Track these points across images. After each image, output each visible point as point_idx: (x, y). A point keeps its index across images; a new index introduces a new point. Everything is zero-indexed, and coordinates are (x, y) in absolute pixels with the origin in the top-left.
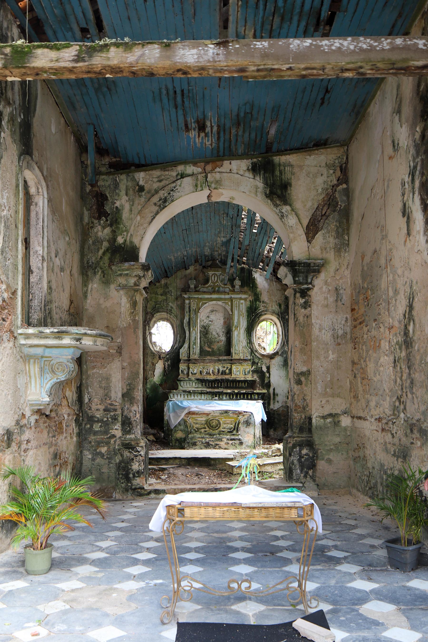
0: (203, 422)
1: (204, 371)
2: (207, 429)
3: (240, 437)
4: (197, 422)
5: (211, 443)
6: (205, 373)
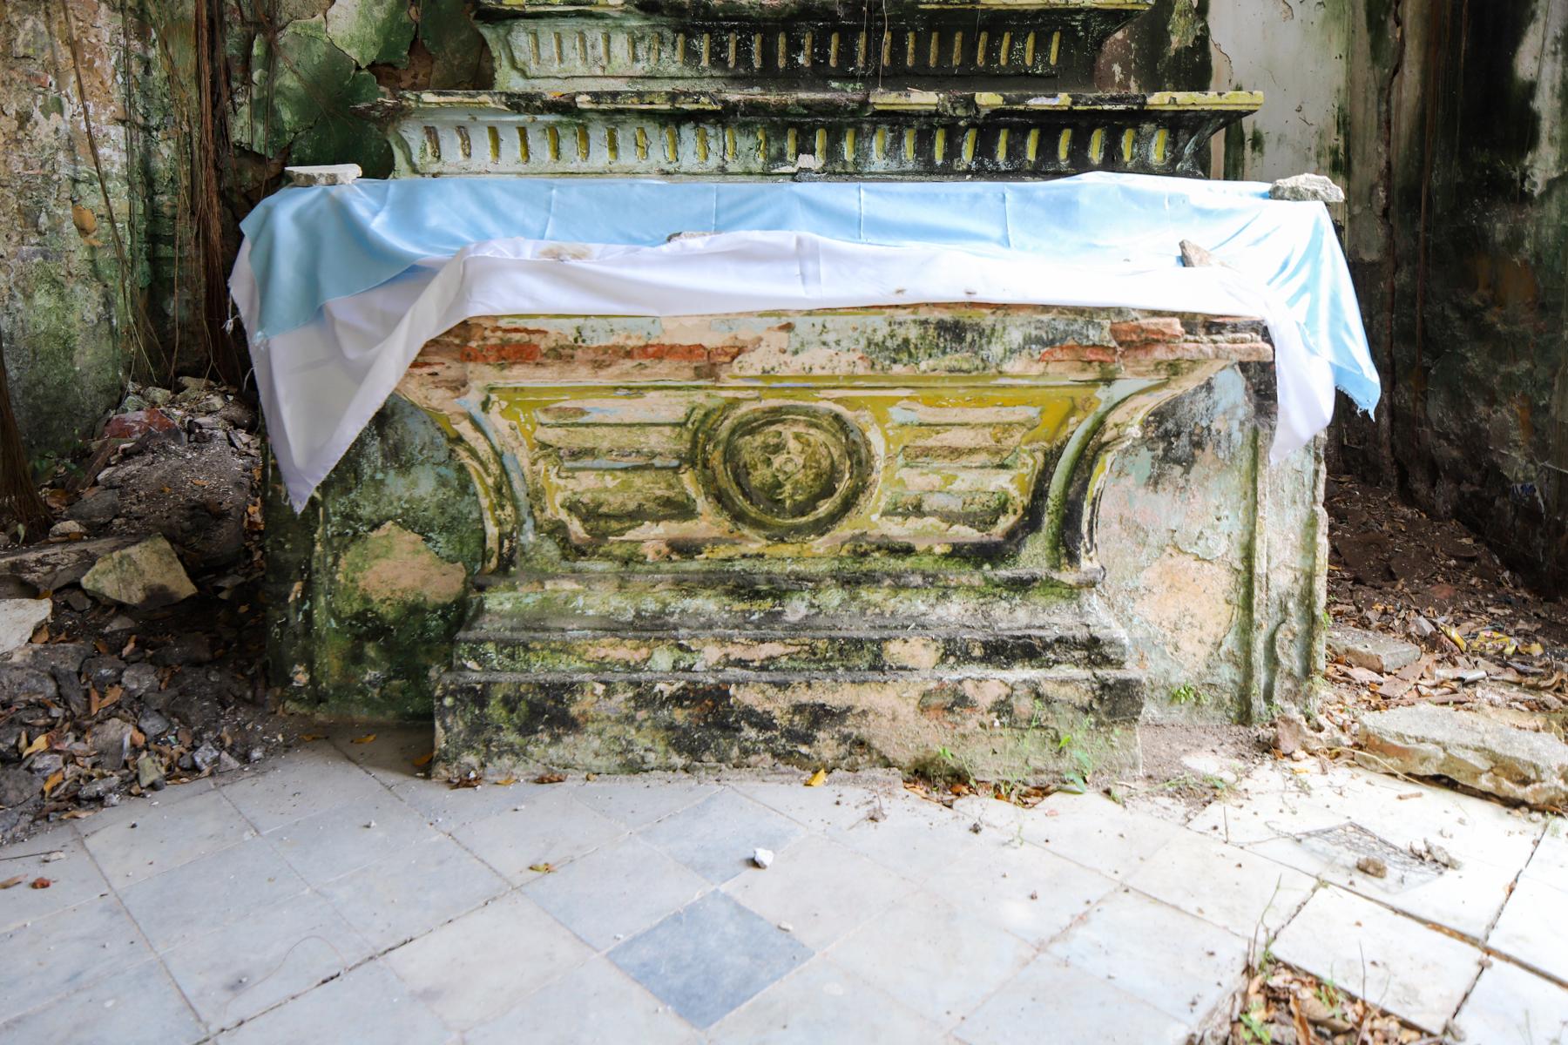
0: (655, 440)
2: (707, 523)
3: (1101, 618)
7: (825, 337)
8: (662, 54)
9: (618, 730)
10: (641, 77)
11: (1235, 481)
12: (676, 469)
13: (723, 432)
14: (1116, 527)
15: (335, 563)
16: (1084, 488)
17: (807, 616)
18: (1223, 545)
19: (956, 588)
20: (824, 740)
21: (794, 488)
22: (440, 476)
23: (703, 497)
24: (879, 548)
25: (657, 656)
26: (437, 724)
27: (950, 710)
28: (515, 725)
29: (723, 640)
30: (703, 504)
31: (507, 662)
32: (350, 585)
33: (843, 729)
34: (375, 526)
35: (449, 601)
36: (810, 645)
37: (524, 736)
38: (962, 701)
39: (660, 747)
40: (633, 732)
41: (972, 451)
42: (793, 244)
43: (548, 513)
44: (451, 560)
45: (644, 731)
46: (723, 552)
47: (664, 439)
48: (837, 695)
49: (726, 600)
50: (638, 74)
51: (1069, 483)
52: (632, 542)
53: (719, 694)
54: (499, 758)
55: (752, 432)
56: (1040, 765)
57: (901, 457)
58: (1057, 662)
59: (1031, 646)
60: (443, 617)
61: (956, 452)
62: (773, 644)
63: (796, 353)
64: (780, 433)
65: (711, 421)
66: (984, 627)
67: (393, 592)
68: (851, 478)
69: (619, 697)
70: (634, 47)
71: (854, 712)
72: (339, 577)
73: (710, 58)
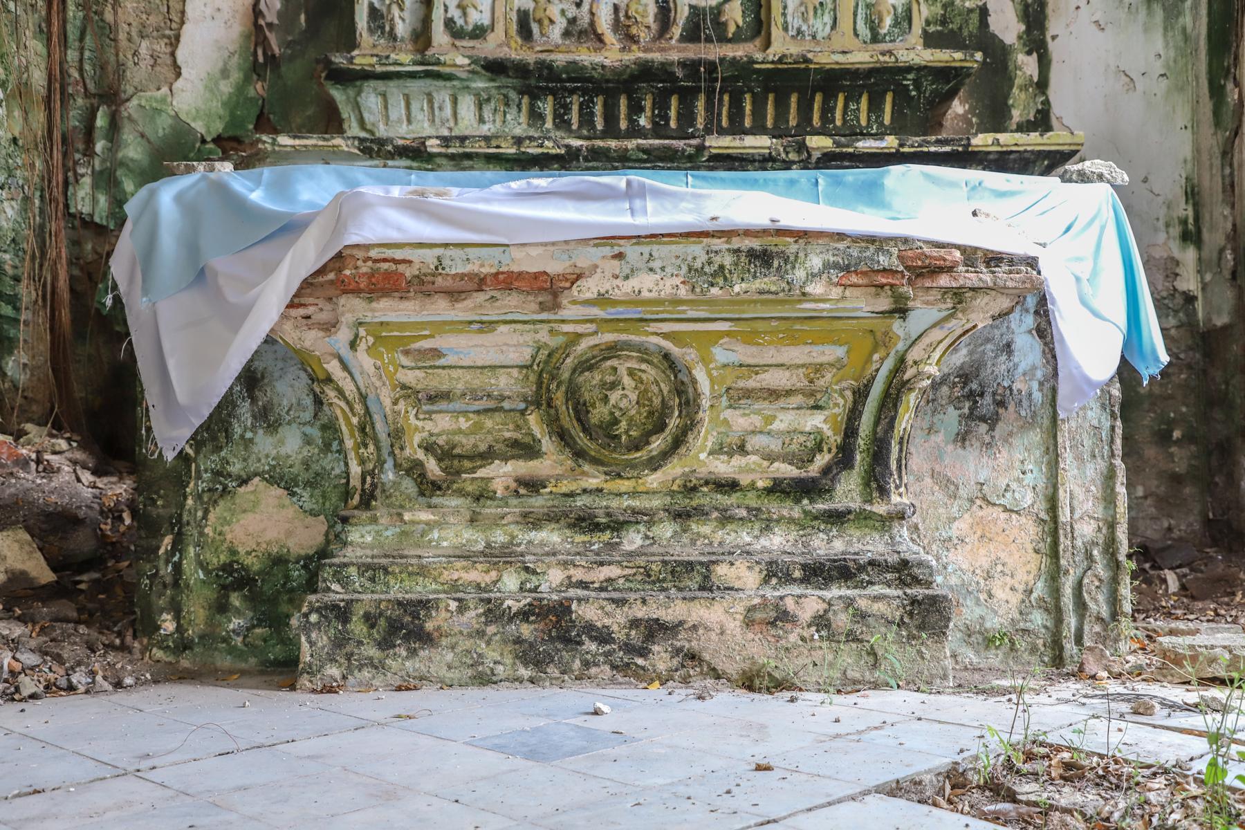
0: (505, 383)
4: (440, 381)
5: (589, 612)
6: (556, 33)
7: (651, 264)
8: (508, 116)
9: (468, 644)
11: (1035, 437)
12: (523, 412)
13: (566, 375)
14: (928, 480)
15: (205, 517)
16: (891, 426)
17: (642, 546)
18: (1029, 499)
19: (778, 521)
20: (659, 653)
21: (628, 425)
22: (305, 435)
23: (547, 438)
24: (707, 483)
25: (505, 578)
26: (303, 639)
27: (773, 624)
28: (375, 640)
29: (565, 564)
30: (547, 444)
31: (368, 584)
32: (218, 538)
33: (675, 643)
34: (244, 482)
35: (311, 552)
36: (645, 568)
37: (383, 650)
38: (783, 617)
39: (508, 660)
40: (483, 645)
41: (789, 393)
42: (623, 185)
43: (408, 452)
44: (313, 513)
45: (494, 645)
46: (565, 487)
47: (513, 381)
48: (670, 611)
49: (568, 532)
51: (877, 422)
52: (482, 479)
53: (562, 610)
54: (360, 670)
55: (590, 368)
56: (857, 675)
57: (725, 398)
58: (871, 583)
59: (847, 568)
60: (305, 567)
61: (774, 394)
62: (611, 567)
63: (627, 278)
64: (615, 369)
65: (554, 361)
66: (803, 553)
67: (258, 544)
68: (680, 416)
69: (472, 613)
70: (480, 109)
71: (686, 626)
72: (206, 530)
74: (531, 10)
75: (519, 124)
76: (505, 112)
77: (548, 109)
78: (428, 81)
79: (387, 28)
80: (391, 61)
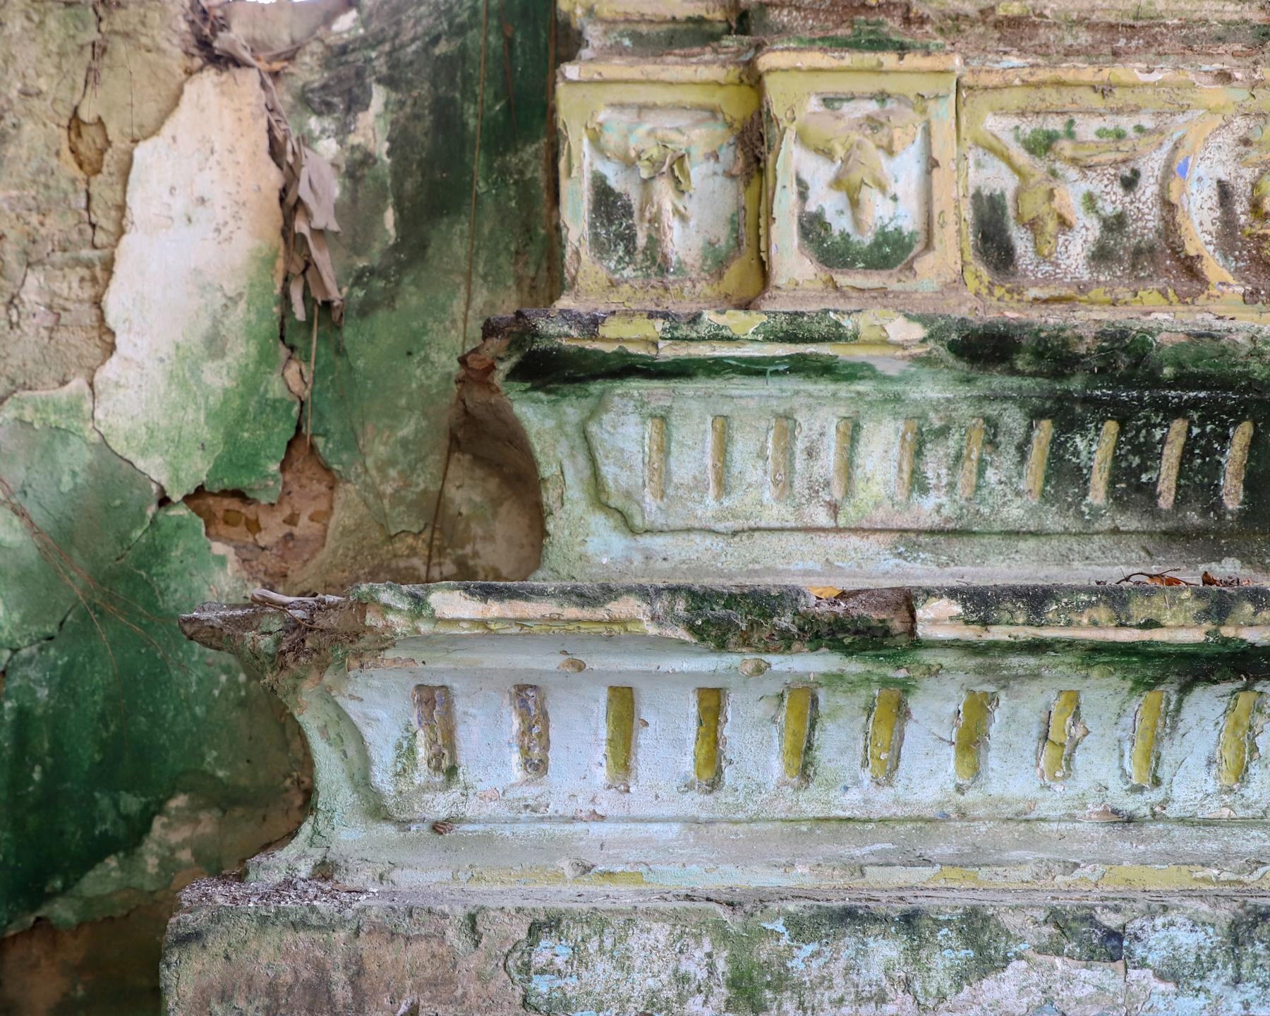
1: (1071, 195)
8: (991, 475)
10: (931, 532)
50: (926, 523)
70: (919, 454)
73: (1112, 483)
74: (1009, 195)
75: (1018, 494)
76: (981, 461)
77: (1098, 457)
78: (791, 384)
79: (641, 241)
80: (703, 330)
